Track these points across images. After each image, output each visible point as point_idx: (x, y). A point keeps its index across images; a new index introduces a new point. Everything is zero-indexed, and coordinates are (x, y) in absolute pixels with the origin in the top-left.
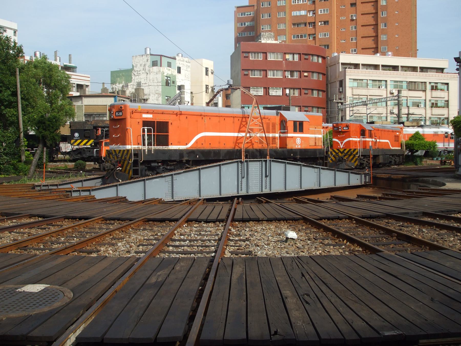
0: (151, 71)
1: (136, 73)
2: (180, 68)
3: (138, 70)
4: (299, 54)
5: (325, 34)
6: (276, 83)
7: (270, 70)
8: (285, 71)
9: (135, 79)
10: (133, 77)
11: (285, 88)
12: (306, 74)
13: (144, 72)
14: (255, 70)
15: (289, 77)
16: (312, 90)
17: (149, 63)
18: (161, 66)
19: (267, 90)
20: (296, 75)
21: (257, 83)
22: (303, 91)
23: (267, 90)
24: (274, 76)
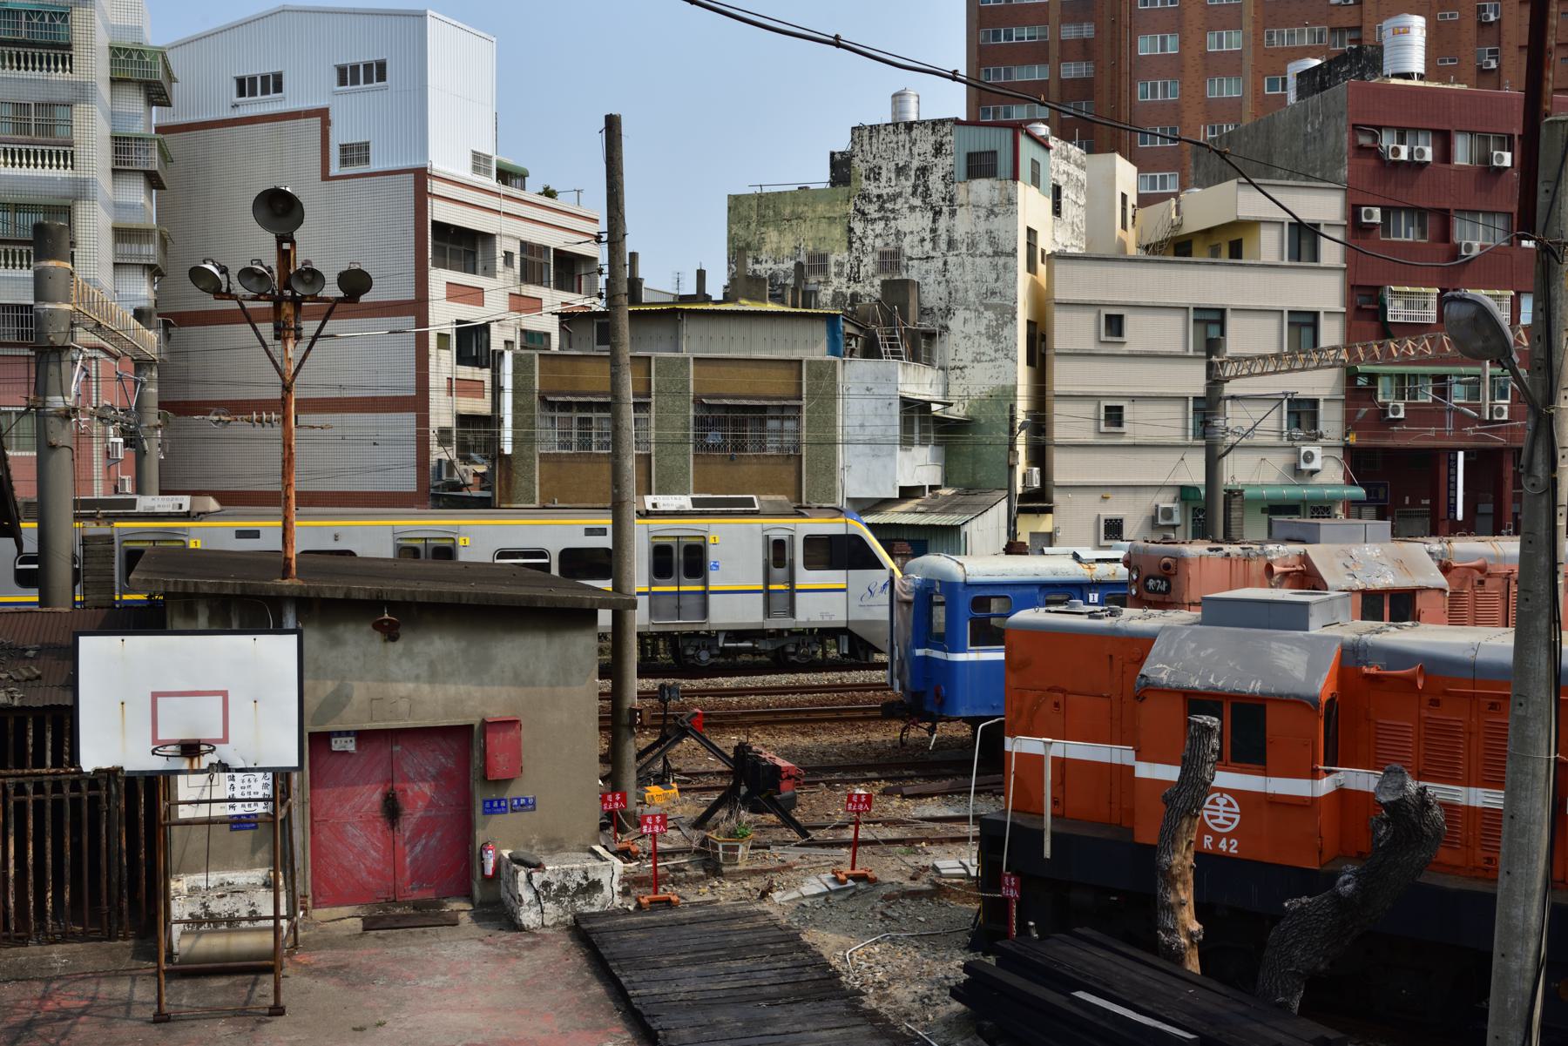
0: (961, 197)
1: (871, 209)
13: (917, 202)
18: (1015, 178)
21: (1408, 268)
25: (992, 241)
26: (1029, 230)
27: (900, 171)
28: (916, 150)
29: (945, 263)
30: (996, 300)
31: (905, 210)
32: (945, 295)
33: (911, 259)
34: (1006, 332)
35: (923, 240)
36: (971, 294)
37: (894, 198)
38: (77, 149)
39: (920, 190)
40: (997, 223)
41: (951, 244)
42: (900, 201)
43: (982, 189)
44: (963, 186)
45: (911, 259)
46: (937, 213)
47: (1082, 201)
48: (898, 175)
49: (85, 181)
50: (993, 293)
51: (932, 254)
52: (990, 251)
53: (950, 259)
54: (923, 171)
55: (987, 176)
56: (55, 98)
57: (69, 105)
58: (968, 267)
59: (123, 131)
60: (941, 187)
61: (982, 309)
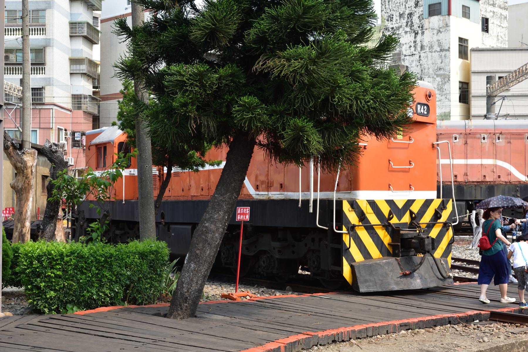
0: (426, 26)
2: (487, 20)
13: (408, 29)
18: (449, 14)
25: (440, 45)
26: (461, 39)
27: (401, 15)
28: (407, 6)
29: (420, 57)
30: (441, 72)
31: (403, 34)
32: (420, 71)
33: (405, 56)
34: (446, 87)
35: (410, 47)
36: (431, 70)
37: (398, 28)
38: (47, 27)
39: (409, 23)
40: (441, 36)
41: (422, 47)
42: (401, 29)
43: (435, 20)
44: (427, 20)
45: (405, 56)
46: (416, 34)
47: (505, 24)
48: (400, 18)
49: (50, 39)
50: (440, 69)
51: (414, 53)
52: (438, 49)
53: (422, 55)
54: (411, 14)
55: (437, 15)
56: (39, 8)
57: (44, 10)
58: (430, 58)
59: (74, 20)
60: (418, 21)
61: (435, 77)
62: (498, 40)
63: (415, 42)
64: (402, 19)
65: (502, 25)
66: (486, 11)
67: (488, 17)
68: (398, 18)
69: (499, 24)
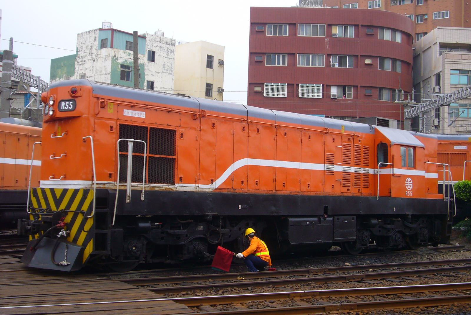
1: (80, 61)
2: (153, 53)
3: (83, 55)
4: (356, 26)
5: (443, 13)
6: (312, 76)
7: (301, 54)
8: (329, 56)
9: (79, 70)
10: (77, 67)
11: (329, 86)
12: (368, 61)
13: (90, 58)
14: (274, 54)
15: (337, 66)
16: (381, 89)
17: (97, 44)
19: (293, 87)
20: (349, 64)
21: (276, 76)
22: (362, 92)
23: (293, 87)
24: (308, 63)
31: (87, 61)
33: (87, 77)
44: (99, 51)
46: (94, 61)
52: (104, 73)
54: (91, 47)
62: (164, 67)
63: (93, 67)
64: (87, 50)
65: (168, 57)
66: (153, 46)
67: (154, 50)
68: (85, 49)
69: (166, 56)
